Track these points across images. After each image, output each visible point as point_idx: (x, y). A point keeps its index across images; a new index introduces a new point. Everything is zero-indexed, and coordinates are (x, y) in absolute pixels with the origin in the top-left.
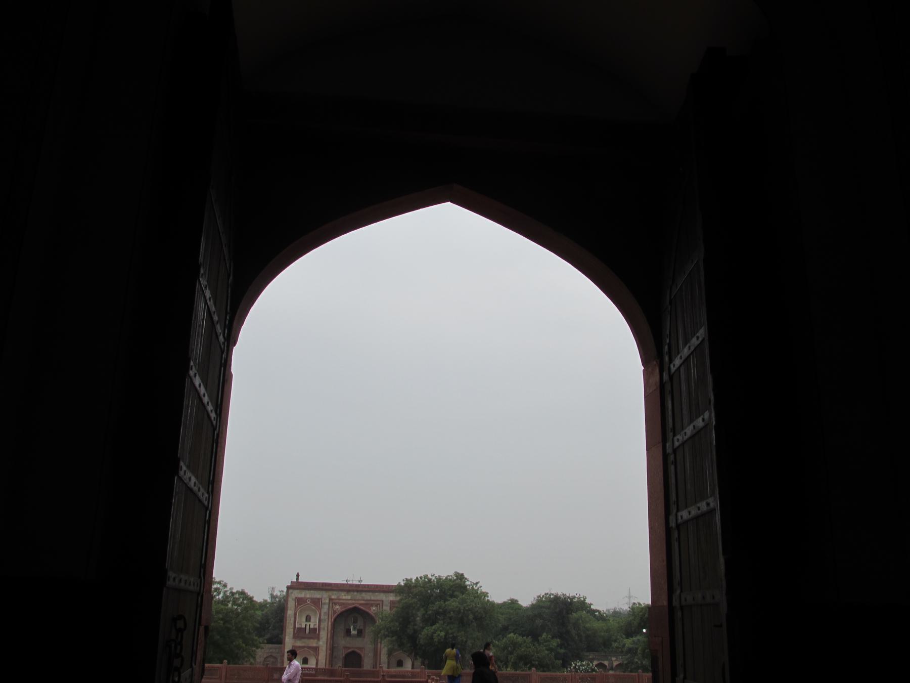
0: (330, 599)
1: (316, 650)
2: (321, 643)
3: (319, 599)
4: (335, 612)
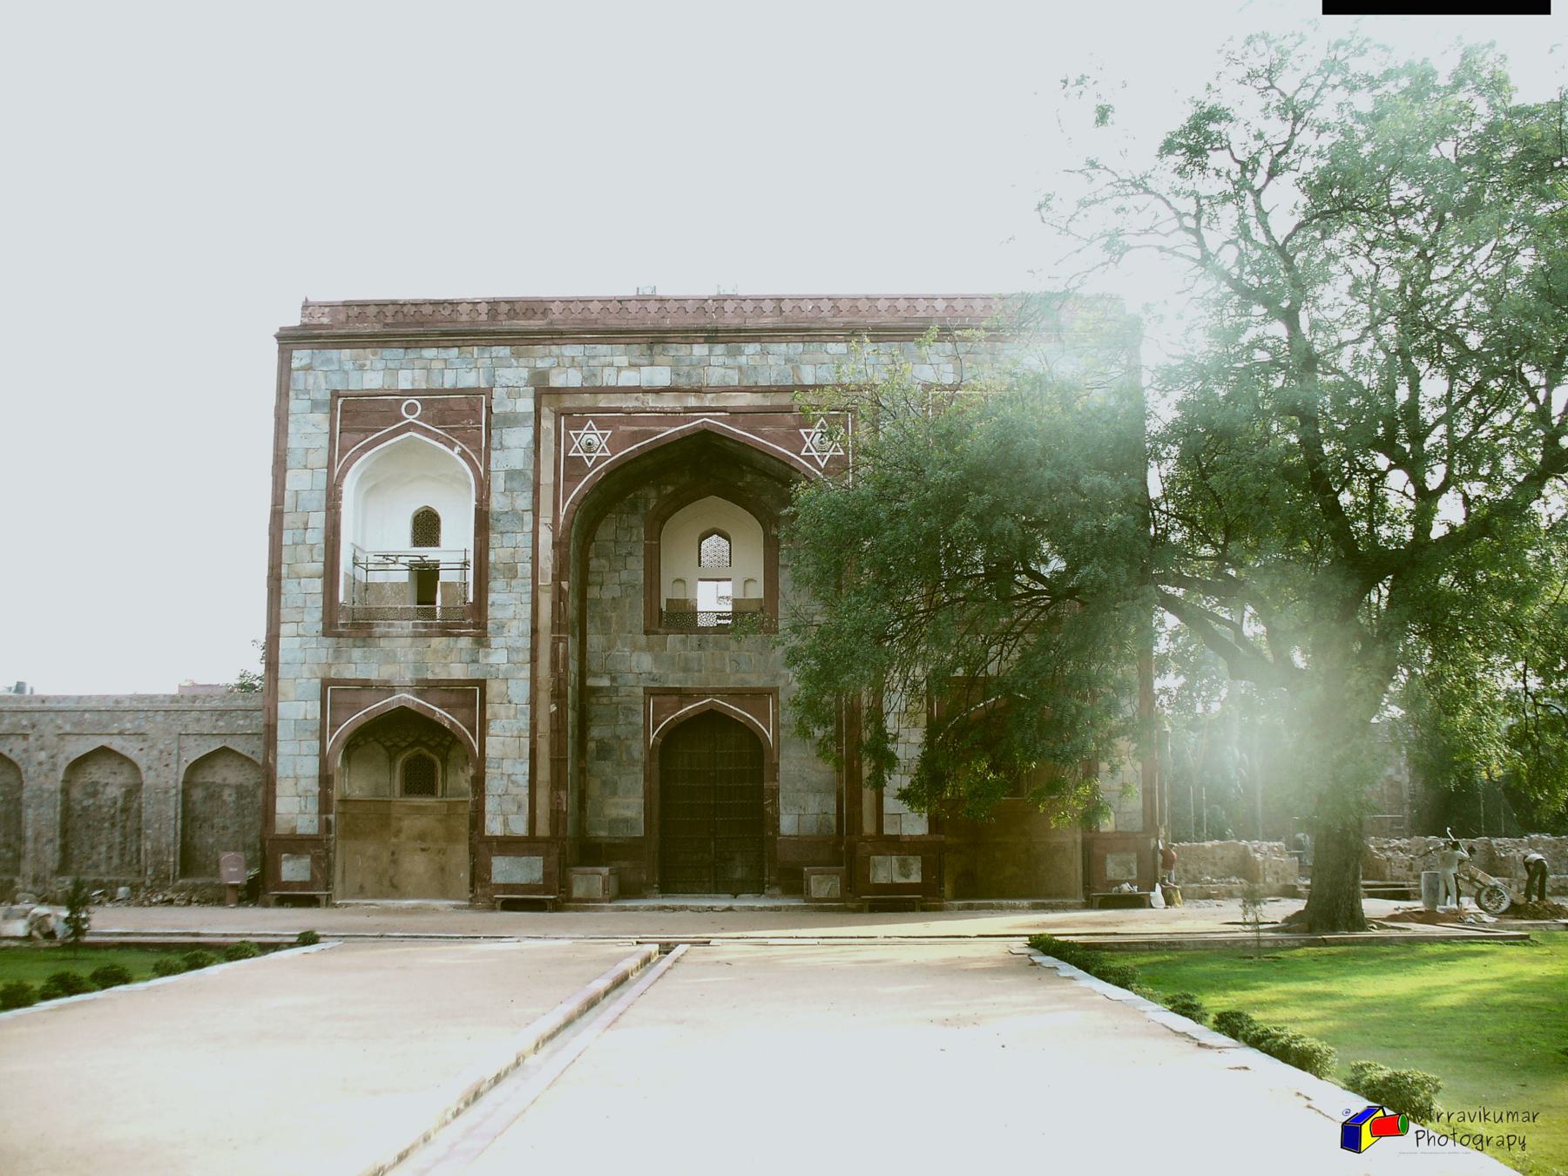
0: (544, 392)
1: (470, 695)
4: (574, 467)
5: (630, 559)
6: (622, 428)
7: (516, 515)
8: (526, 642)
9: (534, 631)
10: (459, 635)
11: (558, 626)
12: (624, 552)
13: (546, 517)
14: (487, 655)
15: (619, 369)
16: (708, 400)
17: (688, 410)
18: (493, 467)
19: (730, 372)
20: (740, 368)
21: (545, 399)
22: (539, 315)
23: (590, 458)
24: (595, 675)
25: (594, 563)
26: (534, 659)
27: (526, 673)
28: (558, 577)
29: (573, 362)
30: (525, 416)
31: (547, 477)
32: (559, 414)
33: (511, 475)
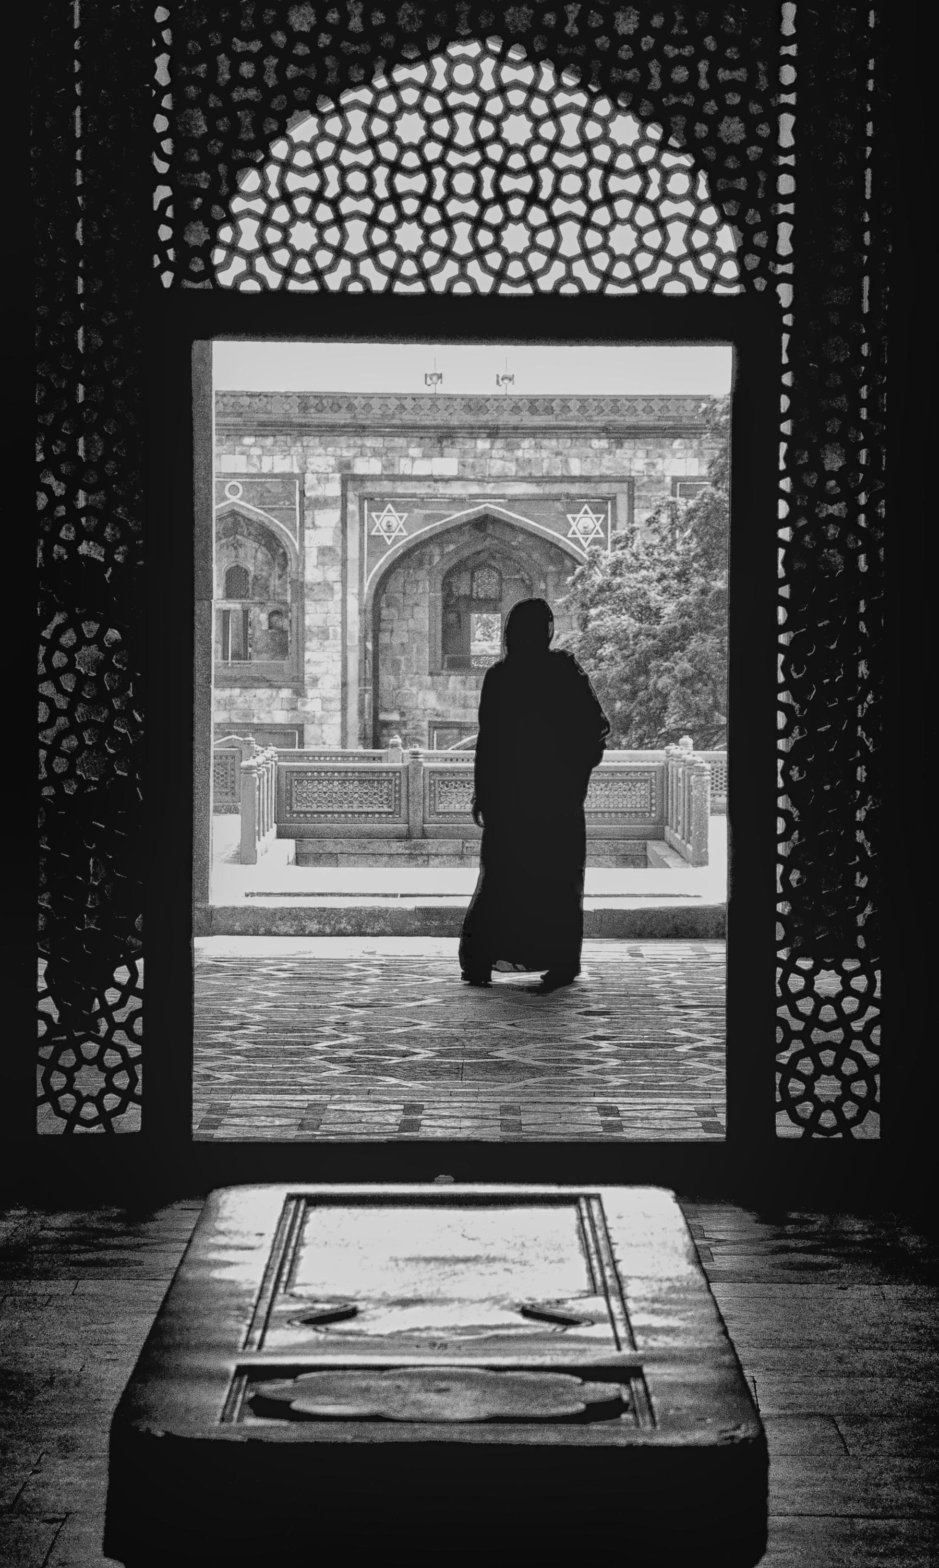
0: (349, 479)
2: (312, 705)
3: (287, 478)
4: (377, 543)
5: (416, 609)
6: (416, 511)
7: (327, 586)
8: (337, 693)
9: (344, 684)
10: (280, 688)
11: (362, 680)
12: (411, 602)
13: (353, 588)
14: (304, 704)
15: (413, 459)
16: (489, 489)
17: (473, 496)
18: (306, 543)
19: (508, 464)
20: (517, 460)
21: (350, 485)
22: (343, 410)
23: (389, 537)
24: (386, 710)
25: (384, 612)
26: (344, 709)
27: (338, 719)
28: (363, 639)
29: (376, 453)
30: (335, 500)
31: (353, 553)
32: (362, 499)
33: (324, 551)
